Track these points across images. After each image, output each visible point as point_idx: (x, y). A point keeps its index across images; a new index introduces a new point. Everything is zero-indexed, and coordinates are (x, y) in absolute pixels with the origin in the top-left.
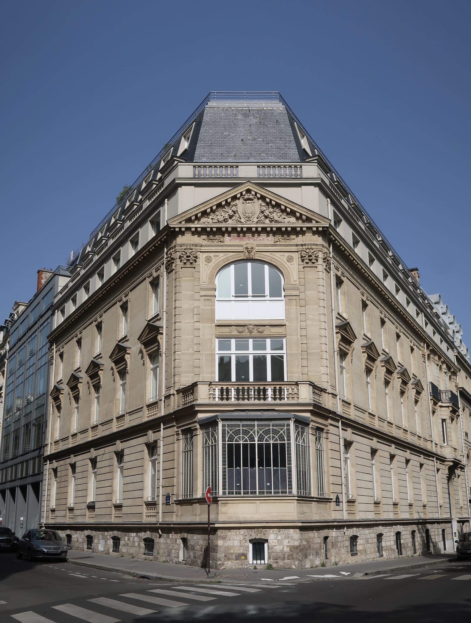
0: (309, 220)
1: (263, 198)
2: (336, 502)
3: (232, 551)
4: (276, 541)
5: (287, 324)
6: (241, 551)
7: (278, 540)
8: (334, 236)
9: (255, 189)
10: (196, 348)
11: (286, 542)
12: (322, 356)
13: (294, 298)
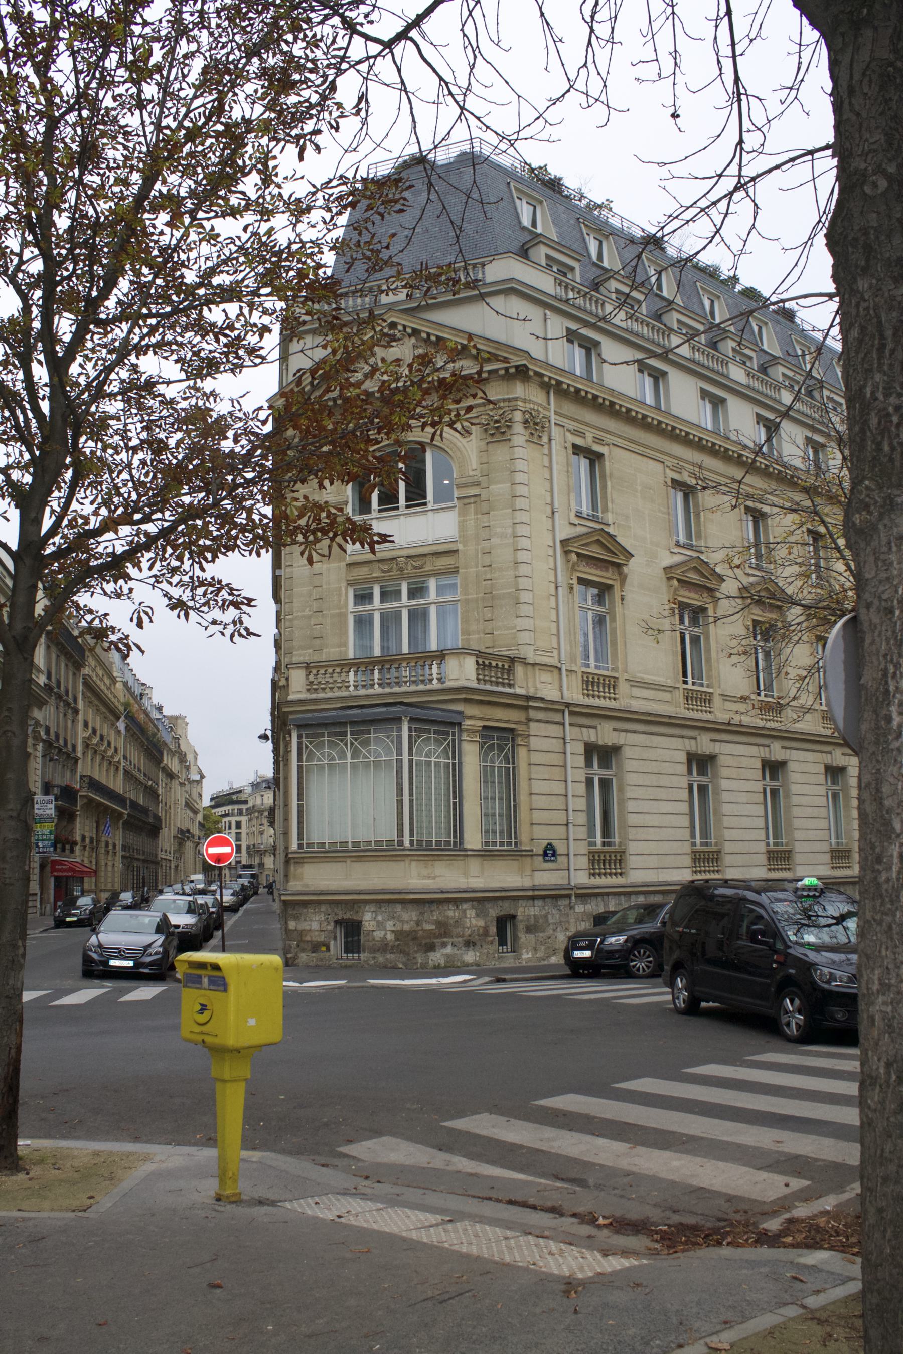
0: (494, 357)
1: (416, 332)
2: (545, 854)
3: (308, 938)
4: (374, 923)
5: (460, 547)
6: (322, 939)
7: (378, 922)
8: (550, 378)
9: (401, 320)
10: (315, 606)
11: (389, 925)
12: (517, 598)
13: (472, 500)
